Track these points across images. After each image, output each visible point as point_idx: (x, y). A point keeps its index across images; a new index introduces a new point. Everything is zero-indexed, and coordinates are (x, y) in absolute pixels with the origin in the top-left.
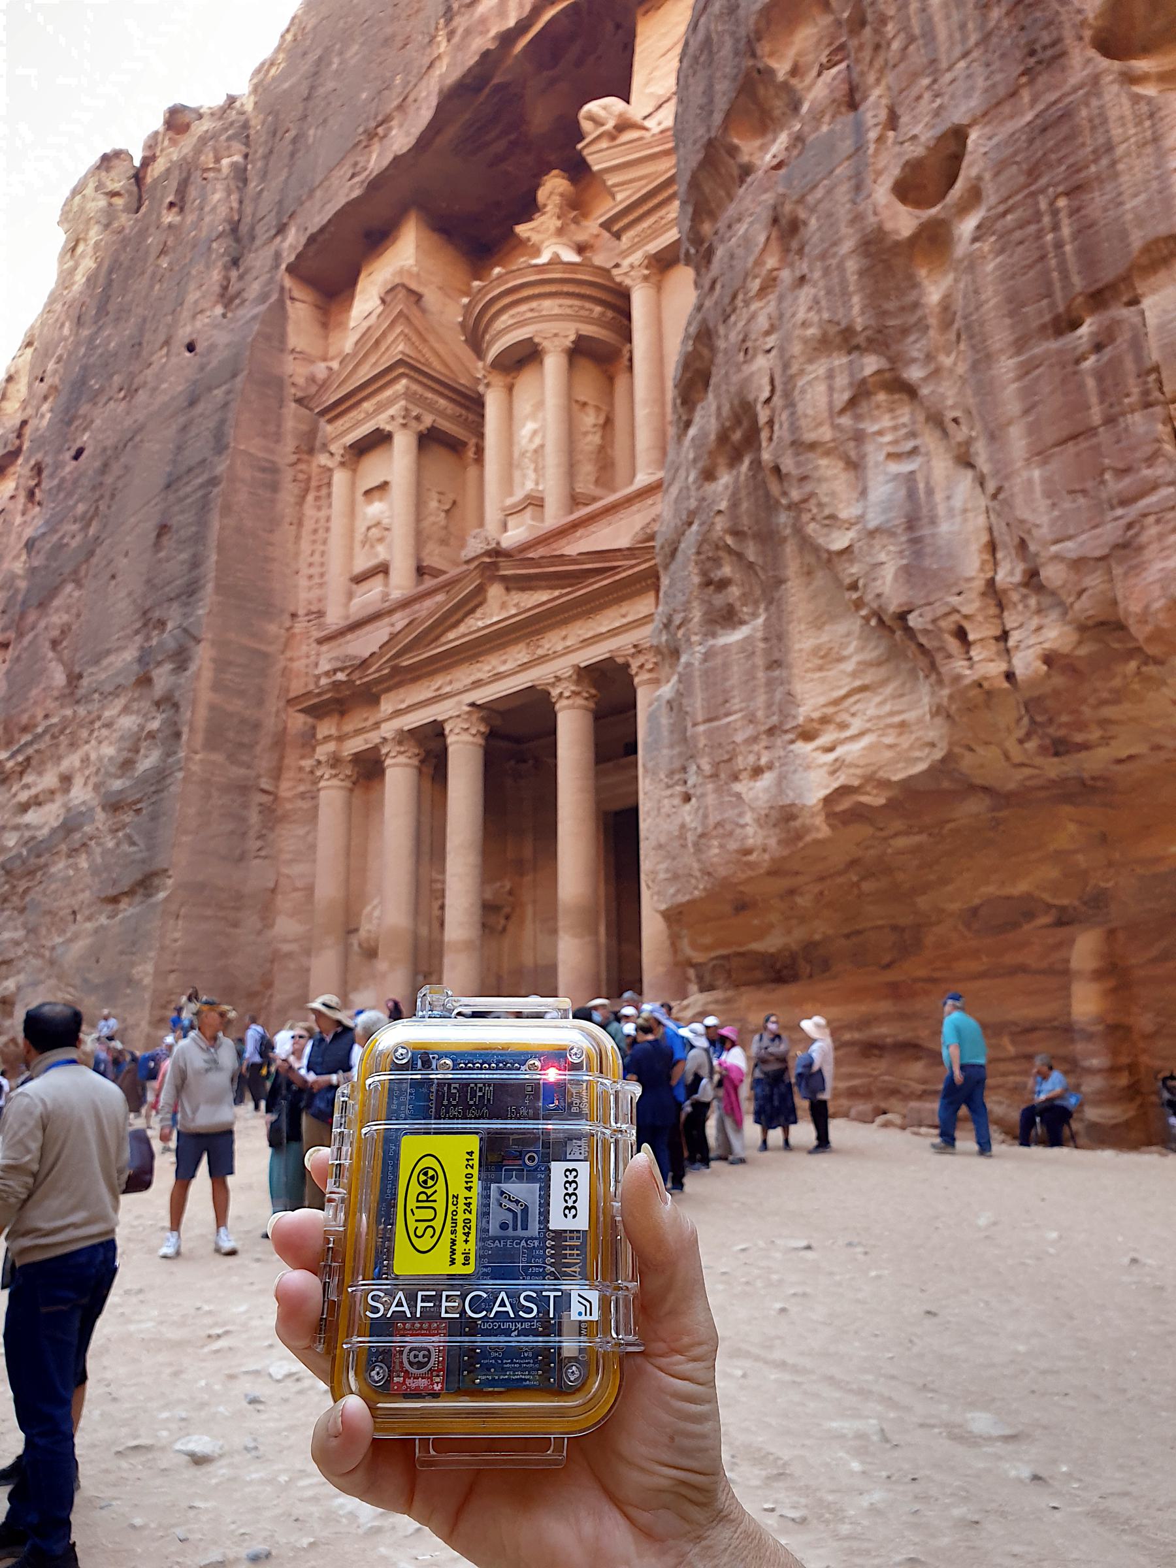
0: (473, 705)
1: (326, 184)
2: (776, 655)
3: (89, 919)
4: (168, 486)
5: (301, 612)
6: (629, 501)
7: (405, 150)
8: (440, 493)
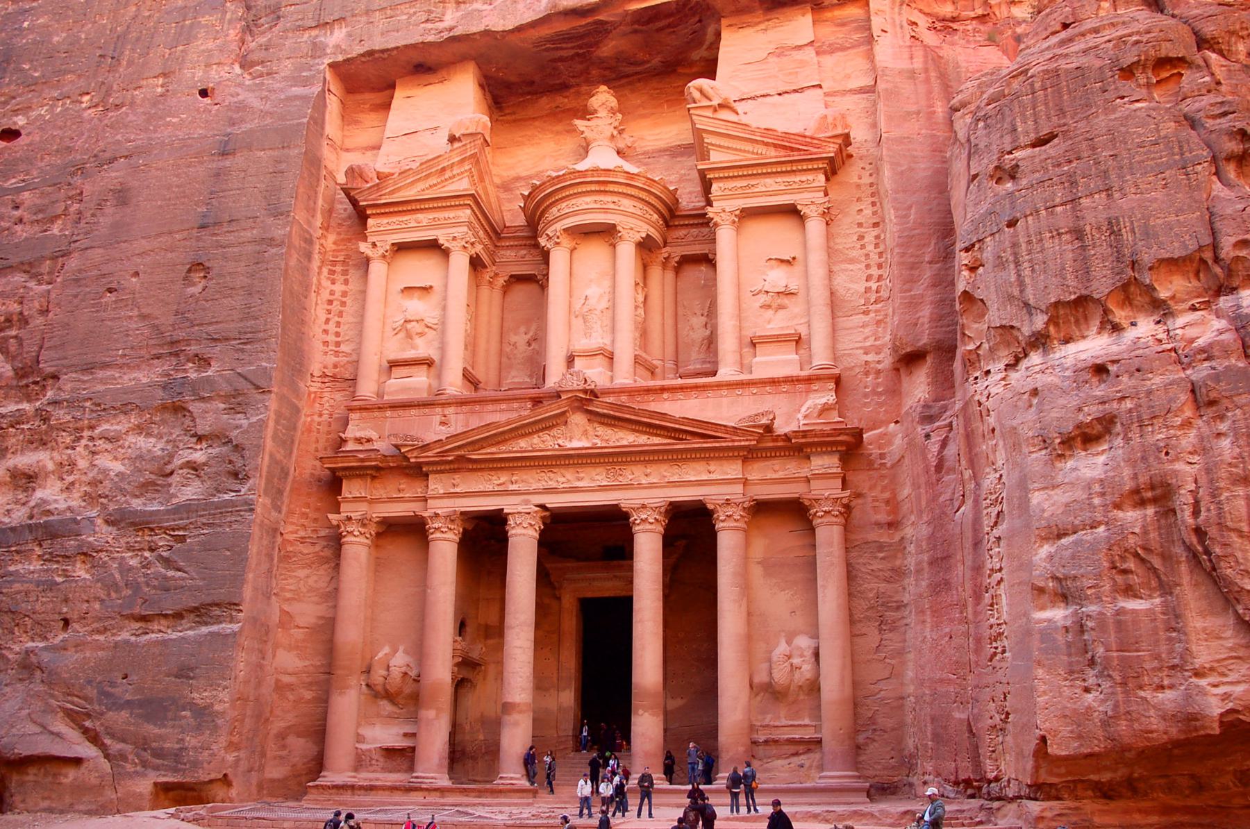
0: (543, 507)
1: (389, 12)
2: (1173, 624)
3: (99, 632)
4: (202, 227)
5: (317, 373)
6: (719, 386)
7: (500, 29)
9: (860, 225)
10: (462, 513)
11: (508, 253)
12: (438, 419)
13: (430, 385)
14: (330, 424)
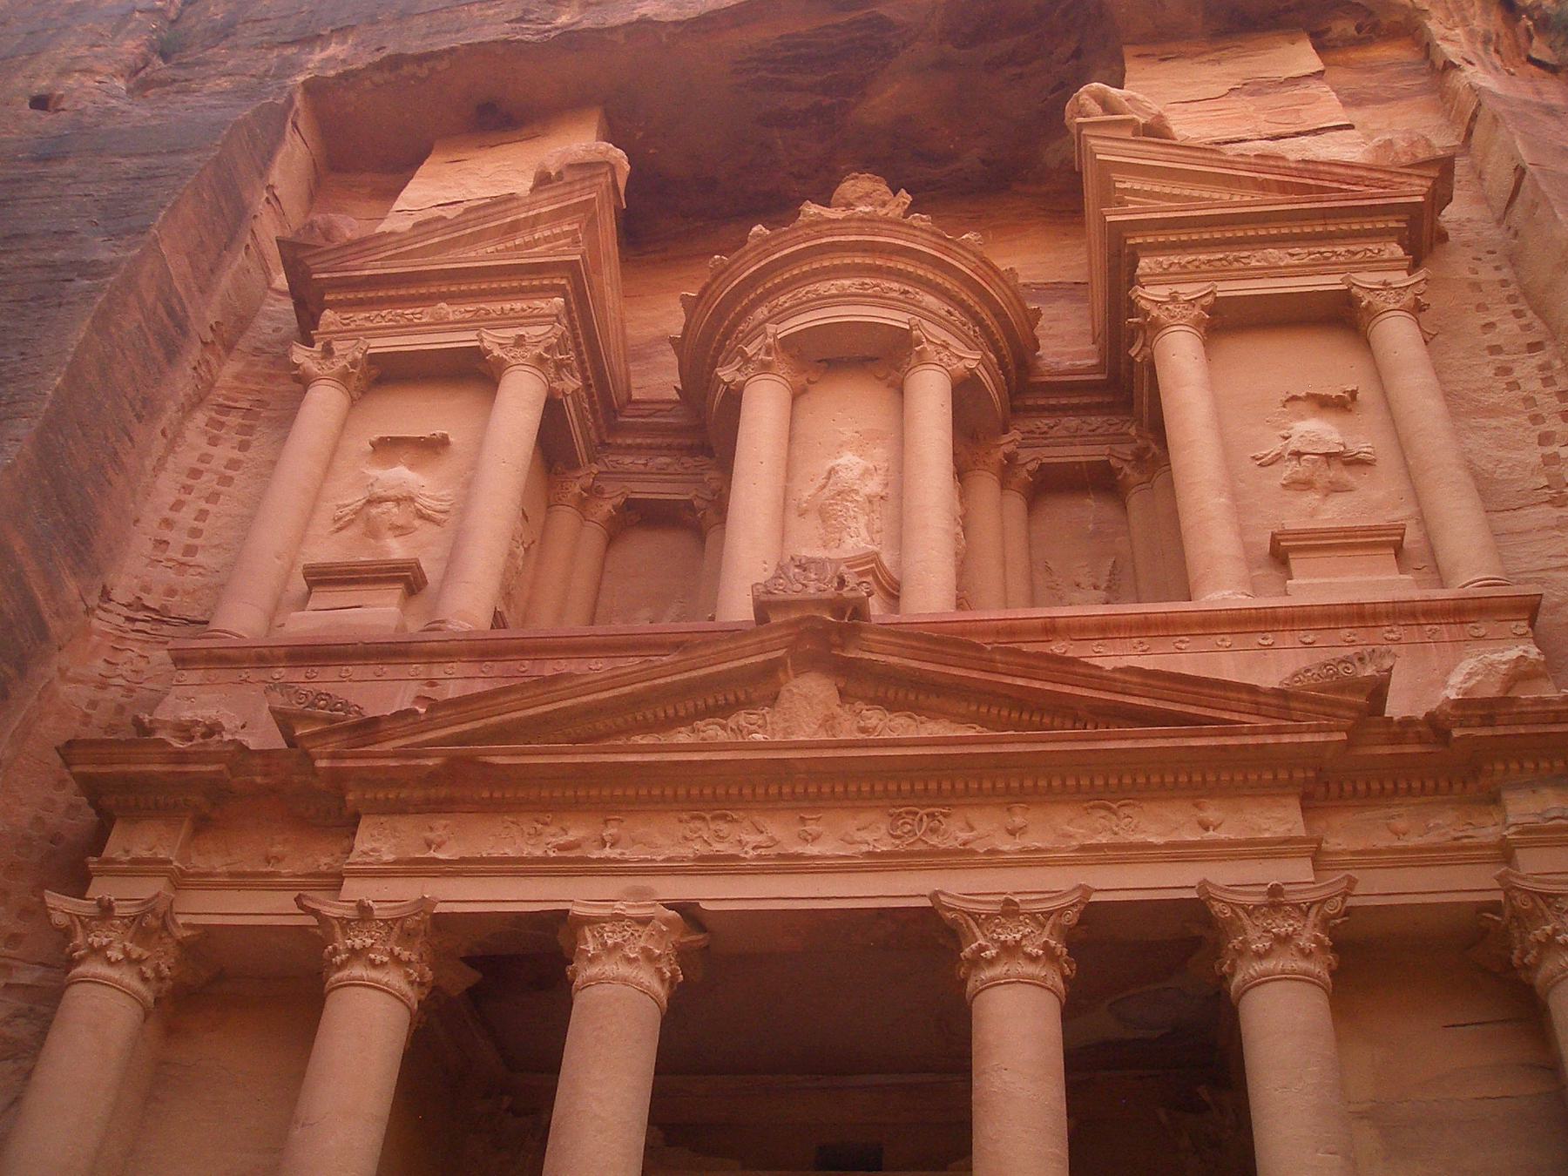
0: (688, 911)
5: (119, 595)
8: (525, 516)
9: (1495, 350)
10: (443, 924)
11: (628, 460)
12: (415, 688)
13: (402, 628)
14: (121, 709)
